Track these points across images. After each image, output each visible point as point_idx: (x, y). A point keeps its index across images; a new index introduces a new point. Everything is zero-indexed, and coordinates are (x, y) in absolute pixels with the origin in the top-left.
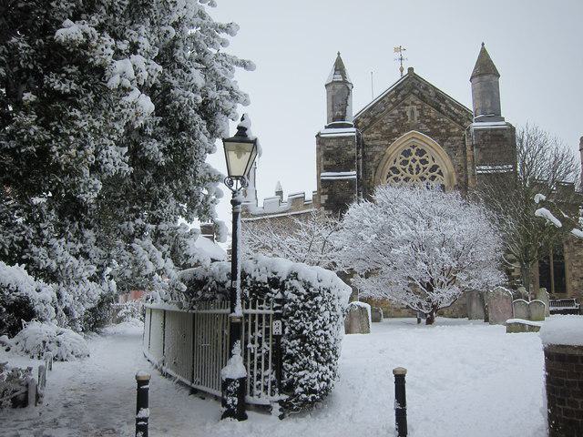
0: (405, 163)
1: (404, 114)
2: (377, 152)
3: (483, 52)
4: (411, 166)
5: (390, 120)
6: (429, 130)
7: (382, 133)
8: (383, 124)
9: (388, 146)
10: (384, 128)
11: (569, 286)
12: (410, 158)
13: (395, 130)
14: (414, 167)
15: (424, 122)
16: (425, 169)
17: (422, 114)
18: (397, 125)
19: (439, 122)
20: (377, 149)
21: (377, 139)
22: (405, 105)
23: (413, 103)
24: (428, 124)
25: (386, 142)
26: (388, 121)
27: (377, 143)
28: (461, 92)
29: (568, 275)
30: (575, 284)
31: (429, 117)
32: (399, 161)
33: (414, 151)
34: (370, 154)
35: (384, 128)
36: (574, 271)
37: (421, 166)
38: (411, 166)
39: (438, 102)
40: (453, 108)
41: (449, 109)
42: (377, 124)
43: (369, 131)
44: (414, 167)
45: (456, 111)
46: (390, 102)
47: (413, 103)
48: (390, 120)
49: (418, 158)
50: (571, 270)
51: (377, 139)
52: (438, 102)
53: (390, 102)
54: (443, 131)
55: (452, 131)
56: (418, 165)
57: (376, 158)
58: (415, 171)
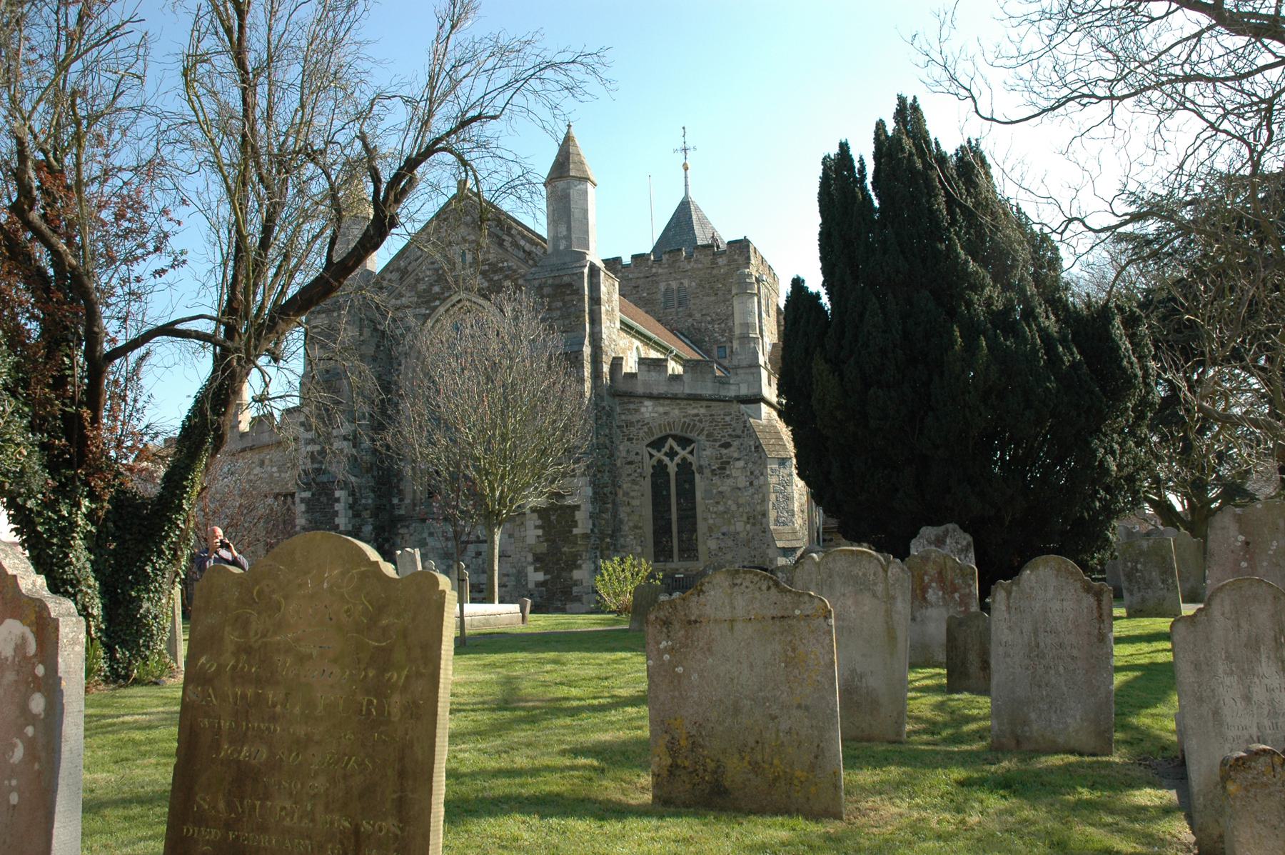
3: (568, 139)
8: (418, 280)
11: (701, 548)
13: (436, 289)
19: (502, 269)
28: (534, 217)
29: (702, 527)
30: (712, 544)
35: (421, 287)
36: (711, 521)
40: (522, 243)
41: (515, 244)
42: (410, 280)
45: (528, 247)
50: (705, 519)
52: (500, 233)
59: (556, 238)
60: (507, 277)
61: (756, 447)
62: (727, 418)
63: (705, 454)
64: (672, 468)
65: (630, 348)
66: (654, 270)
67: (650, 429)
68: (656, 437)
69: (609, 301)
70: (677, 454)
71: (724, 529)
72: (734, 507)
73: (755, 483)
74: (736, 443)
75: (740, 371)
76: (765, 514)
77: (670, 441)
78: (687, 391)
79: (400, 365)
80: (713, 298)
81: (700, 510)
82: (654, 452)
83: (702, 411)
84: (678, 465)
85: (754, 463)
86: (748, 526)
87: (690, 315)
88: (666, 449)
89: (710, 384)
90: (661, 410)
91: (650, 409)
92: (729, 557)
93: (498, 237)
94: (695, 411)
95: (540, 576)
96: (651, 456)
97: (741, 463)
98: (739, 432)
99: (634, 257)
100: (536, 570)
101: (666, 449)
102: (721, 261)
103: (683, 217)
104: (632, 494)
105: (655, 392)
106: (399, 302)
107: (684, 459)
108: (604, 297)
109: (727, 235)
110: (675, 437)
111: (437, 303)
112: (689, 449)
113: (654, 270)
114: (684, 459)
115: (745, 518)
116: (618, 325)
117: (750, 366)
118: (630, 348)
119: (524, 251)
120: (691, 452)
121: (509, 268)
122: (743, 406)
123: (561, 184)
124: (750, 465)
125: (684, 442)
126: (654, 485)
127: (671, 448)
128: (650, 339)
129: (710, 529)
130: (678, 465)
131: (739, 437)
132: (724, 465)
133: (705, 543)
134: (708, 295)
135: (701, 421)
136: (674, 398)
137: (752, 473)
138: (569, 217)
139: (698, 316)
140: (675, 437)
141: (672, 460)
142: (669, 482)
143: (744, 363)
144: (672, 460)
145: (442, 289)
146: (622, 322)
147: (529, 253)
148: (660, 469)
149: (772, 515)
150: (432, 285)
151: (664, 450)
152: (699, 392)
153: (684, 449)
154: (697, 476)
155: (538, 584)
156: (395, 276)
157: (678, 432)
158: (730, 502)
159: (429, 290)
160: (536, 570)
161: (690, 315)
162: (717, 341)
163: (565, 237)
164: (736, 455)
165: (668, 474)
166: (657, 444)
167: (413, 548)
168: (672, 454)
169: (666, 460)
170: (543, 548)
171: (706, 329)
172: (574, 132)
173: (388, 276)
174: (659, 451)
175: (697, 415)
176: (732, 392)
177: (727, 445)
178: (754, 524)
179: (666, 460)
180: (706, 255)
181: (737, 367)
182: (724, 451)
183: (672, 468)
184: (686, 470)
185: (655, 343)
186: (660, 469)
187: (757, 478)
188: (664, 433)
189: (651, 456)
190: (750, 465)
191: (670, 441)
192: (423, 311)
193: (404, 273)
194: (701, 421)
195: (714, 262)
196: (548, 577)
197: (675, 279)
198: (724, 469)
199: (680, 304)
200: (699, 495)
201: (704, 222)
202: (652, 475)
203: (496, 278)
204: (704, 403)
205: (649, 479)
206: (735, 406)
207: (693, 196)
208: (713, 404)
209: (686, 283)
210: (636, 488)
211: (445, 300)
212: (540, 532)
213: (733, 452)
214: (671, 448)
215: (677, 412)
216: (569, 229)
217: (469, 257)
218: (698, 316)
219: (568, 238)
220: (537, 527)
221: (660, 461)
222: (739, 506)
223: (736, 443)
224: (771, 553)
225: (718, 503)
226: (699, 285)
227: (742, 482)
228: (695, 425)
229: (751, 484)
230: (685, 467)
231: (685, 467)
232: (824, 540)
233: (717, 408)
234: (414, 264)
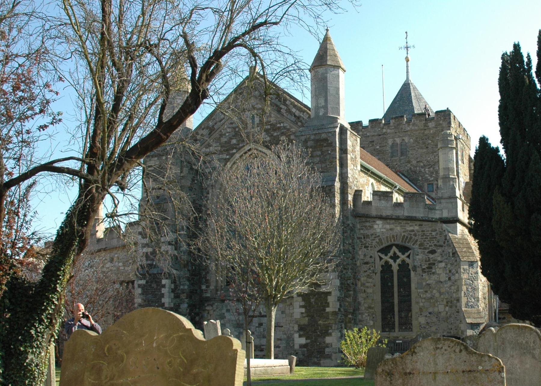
3: (326, 39)
5: (228, 130)
8: (221, 135)
11: (414, 323)
13: (234, 141)
19: (279, 128)
28: (302, 93)
29: (415, 308)
30: (422, 320)
35: (224, 140)
36: (421, 304)
40: (294, 110)
41: (289, 111)
42: (216, 135)
45: (297, 113)
48: (228, 130)
50: (418, 303)
52: (278, 103)
59: (317, 108)
60: (283, 134)
61: (453, 254)
62: (434, 233)
63: (418, 258)
64: (395, 267)
65: (367, 184)
66: (384, 130)
67: (380, 240)
68: (384, 245)
69: (354, 151)
70: (398, 257)
71: (431, 310)
72: (437, 295)
73: (453, 278)
74: (439, 251)
75: (442, 201)
76: (458, 300)
77: (394, 249)
78: (406, 214)
79: (208, 193)
80: (425, 150)
81: (414, 296)
82: (383, 256)
83: (417, 228)
84: (399, 265)
85: (452, 264)
86: (447, 308)
87: (409, 162)
88: (391, 254)
89: (422, 210)
90: (388, 227)
91: (380, 226)
92: (433, 329)
93: (277, 106)
94: (411, 228)
95: (303, 341)
96: (381, 258)
97: (443, 265)
98: (441, 243)
99: (371, 121)
100: (300, 336)
101: (391, 254)
102: (431, 125)
103: (405, 94)
104: (367, 285)
105: (384, 215)
106: (208, 150)
107: (403, 261)
108: (349, 148)
109: (435, 107)
110: (397, 246)
111: (234, 151)
112: (407, 254)
113: (384, 130)
114: (403, 261)
115: (445, 303)
116: (359, 168)
117: (450, 198)
118: (367, 184)
119: (295, 116)
120: (408, 257)
121: (285, 127)
122: (444, 225)
123: (321, 70)
124: (449, 266)
125: (404, 249)
126: (383, 279)
127: (395, 253)
128: (381, 178)
129: (421, 310)
130: (399, 265)
131: (441, 246)
132: (431, 266)
133: (417, 319)
134: (422, 148)
135: (415, 235)
136: (397, 219)
137: (450, 271)
138: (326, 93)
139: (414, 162)
140: (397, 246)
141: (395, 261)
142: (393, 276)
143: (446, 195)
144: (395, 261)
145: (238, 141)
146: (362, 166)
147: (299, 118)
148: (387, 268)
149: (464, 300)
150: (231, 139)
151: (389, 255)
152: (414, 215)
153: (403, 254)
154: (412, 273)
155: (301, 346)
156: (205, 132)
157: (399, 242)
158: (434, 291)
159: (228, 142)
160: (300, 336)
161: (409, 162)
162: (427, 180)
163: (323, 107)
164: (439, 259)
165: (392, 271)
166: (385, 250)
167: (216, 320)
168: (395, 257)
169: (391, 261)
170: (305, 321)
171: (420, 171)
172: (330, 34)
173: (201, 132)
174: (386, 255)
175: (413, 231)
176: (437, 215)
177: (433, 252)
178: (451, 307)
179: (391, 261)
180: (421, 121)
181: (441, 198)
182: (431, 256)
183: (395, 267)
184: (404, 268)
185: (385, 180)
186: (387, 268)
187: (454, 275)
188: (390, 243)
189: (381, 258)
190: (449, 266)
191: (394, 249)
192: (225, 156)
193: (212, 130)
194: (415, 235)
195: (426, 125)
196: (309, 341)
197: (399, 137)
198: (431, 268)
199: (402, 154)
200: (413, 286)
201: (419, 98)
202: (381, 272)
203: (275, 134)
204: (418, 223)
205: (379, 274)
206: (439, 225)
207: (412, 80)
208: (424, 223)
209: (406, 139)
210: (370, 280)
211: (240, 149)
212: (303, 310)
213: (437, 257)
214: (395, 253)
215: (399, 228)
216: (326, 101)
217: (257, 120)
218: (414, 162)
219: (325, 107)
220: (301, 307)
221: (387, 262)
222: (441, 294)
223: (439, 251)
224: (462, 326)
225: (426, 292)
226: (416, 141)
227: (443, 277)
228: (411, 238)
229: (450, 279)
230: (404, 266)
231: (404, 266)
232: (499, 318)
233: (427, 226)
234: (219, 124)
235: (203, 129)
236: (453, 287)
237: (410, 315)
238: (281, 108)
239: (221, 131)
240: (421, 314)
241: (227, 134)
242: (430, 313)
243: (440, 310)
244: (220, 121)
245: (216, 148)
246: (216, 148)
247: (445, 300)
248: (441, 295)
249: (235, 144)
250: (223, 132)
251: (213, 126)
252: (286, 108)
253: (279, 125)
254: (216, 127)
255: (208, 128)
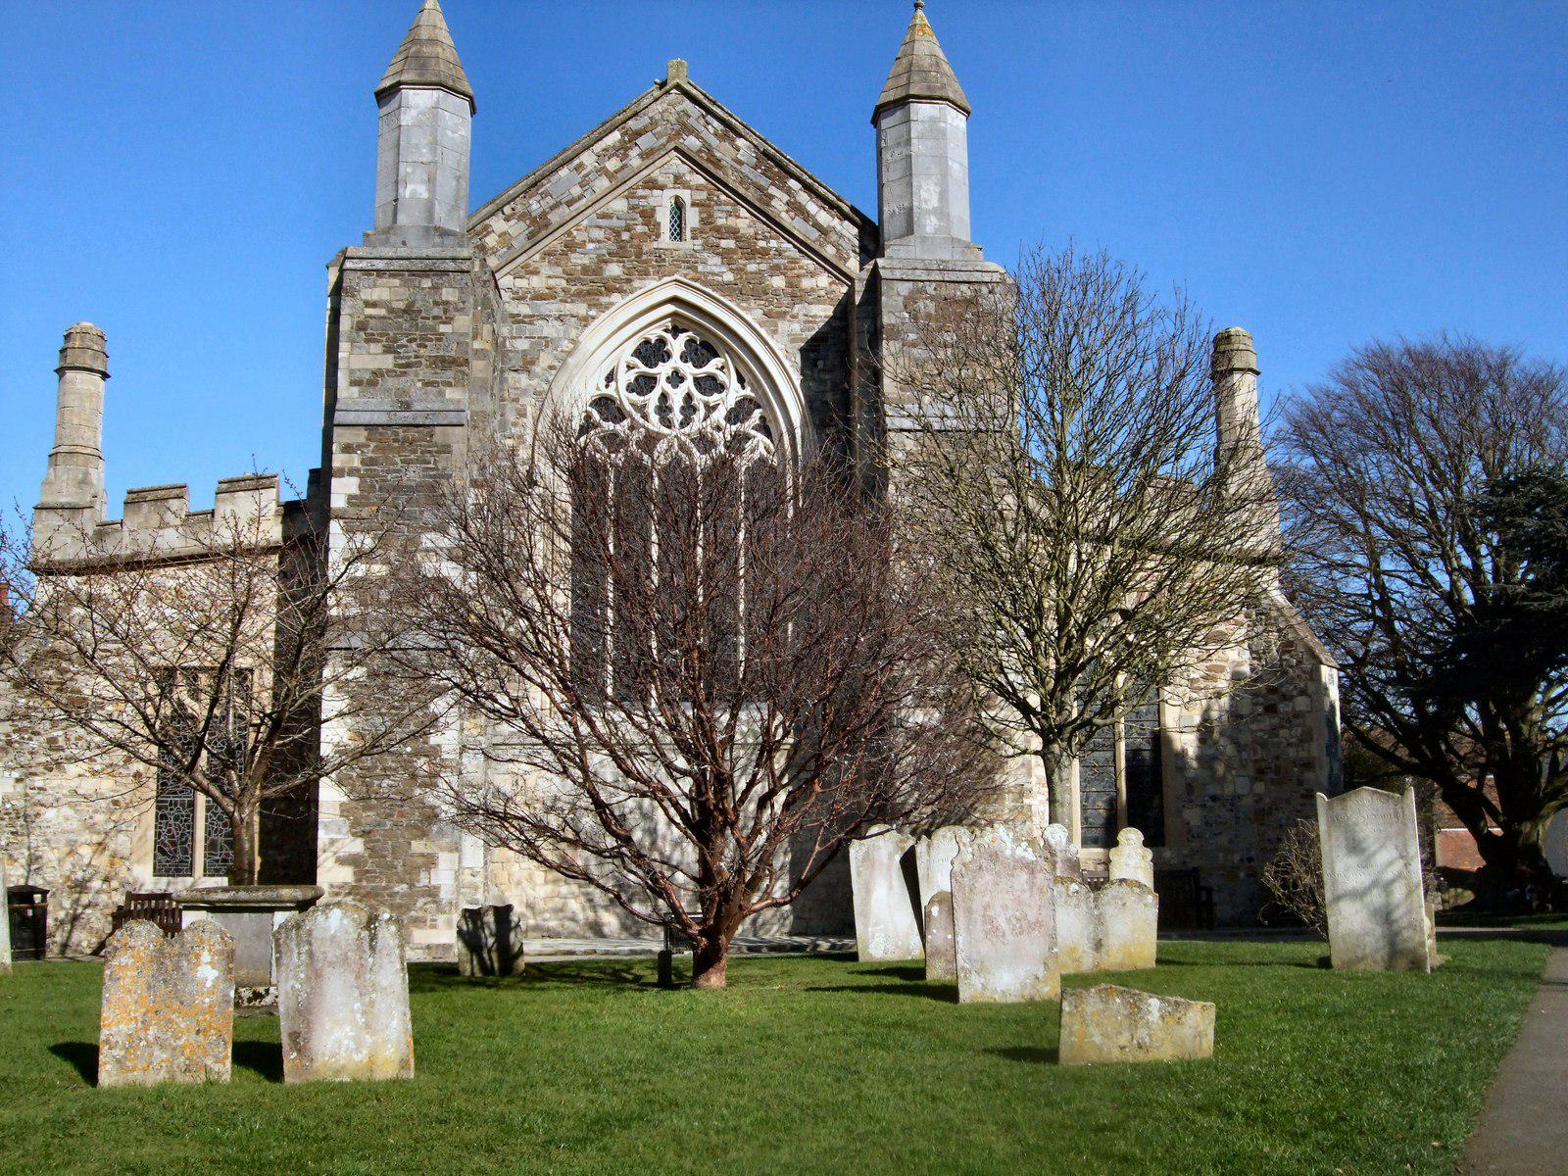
0: (643, 384)
1: (648, 215)
2: (547, 342)
4: (664, 397)
5: (599, 234)
6: (729, 277)
7: (570, 278)
8: (571, 246)
9: (585, 321)
10: (578, 259)
12: (663, 370)
13: (614, 270)
14: (677, 399)
15: (714, 248)
16: (710, 409)
17: (707, 220)
18: (619, 254)
19: (764, 252)
20: (550, 329)
21: (549, 295)
22: (652, 184)
23: (678, 180)
24: (726, 256)
25: (581, 309)
26: (592, 237)
27: (551, 307)
31: (733, 233)
32: (625, 378)
33: (677, 345)
34: (523, 345)
35: (578, 259)
37: (699, 398)
38: (664, 397)
39: (763, 181)
42: (554, 242)
43: (525, 267)
44: (677, 399)
46: (602, 171)
47: (678, 180)
48: (599, 234)
49: (689, 370)
51: (549, 295)
53: (602, 171)
54: (778, 282)
55: (806, 283)
56: (689, 397)
57: (545, 359)
58: (677, 416)
60: (776, 270)
73: (1283, 707)
86: (1260, 787)
92: (1223, 840)
106: (522, 283)
115: (1251, 771)
119: (817, 226)
133: (1179, 812)
150: (603, 261)
159: (595, 270)
163: (935, 211)
203: (752, 267)
217: (692, 217)
234: (565, 212)
235: (507, 219)
236: (1283, 732)
237: (1156, 802)
238: (771, 197)
239: (569, 233)
240: (1191, 801)
241: (590, 246)
242: (1214, 798)
243: (1240, 791)
244: (569, 204)
245: (552, 282)
246: (552, 282)
247: (1250, 765)
248: (1239, 752)
249: (616, 279)
250: (579, 237)
251: (544, 215)
252: (786, 198)
253: (762, 244)
254: (555, 218)
255: (522, 217)
